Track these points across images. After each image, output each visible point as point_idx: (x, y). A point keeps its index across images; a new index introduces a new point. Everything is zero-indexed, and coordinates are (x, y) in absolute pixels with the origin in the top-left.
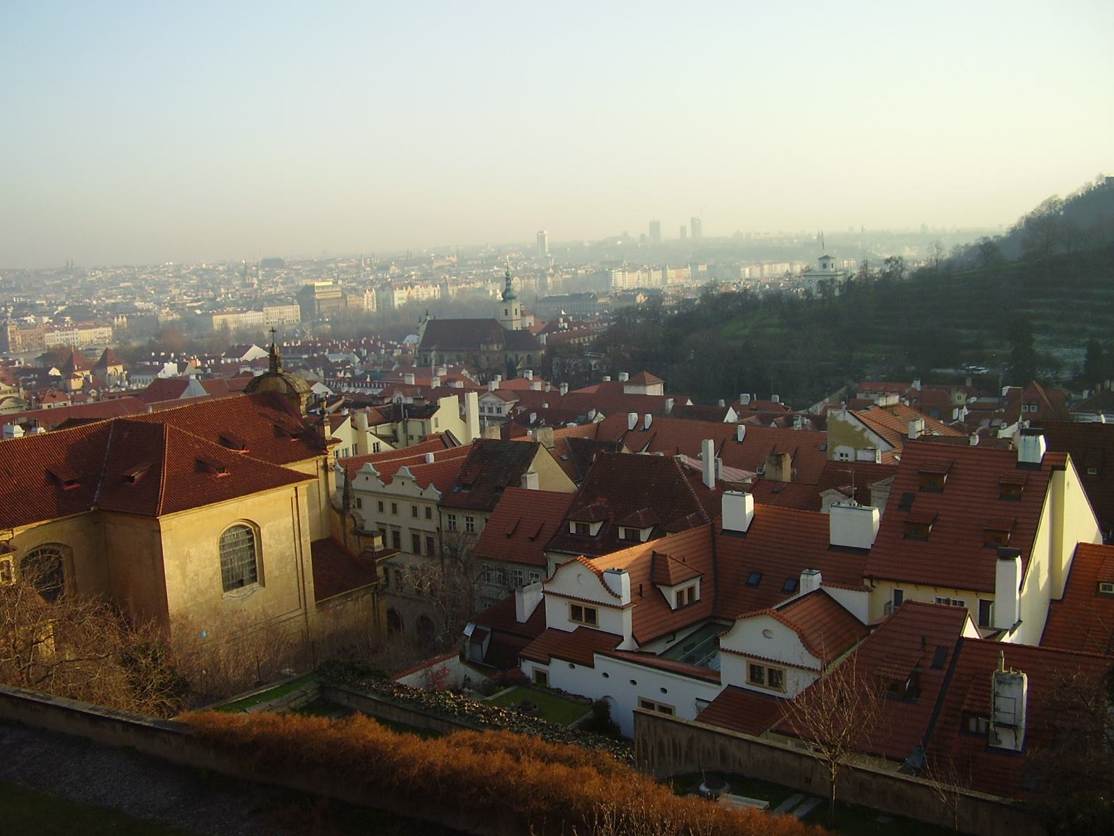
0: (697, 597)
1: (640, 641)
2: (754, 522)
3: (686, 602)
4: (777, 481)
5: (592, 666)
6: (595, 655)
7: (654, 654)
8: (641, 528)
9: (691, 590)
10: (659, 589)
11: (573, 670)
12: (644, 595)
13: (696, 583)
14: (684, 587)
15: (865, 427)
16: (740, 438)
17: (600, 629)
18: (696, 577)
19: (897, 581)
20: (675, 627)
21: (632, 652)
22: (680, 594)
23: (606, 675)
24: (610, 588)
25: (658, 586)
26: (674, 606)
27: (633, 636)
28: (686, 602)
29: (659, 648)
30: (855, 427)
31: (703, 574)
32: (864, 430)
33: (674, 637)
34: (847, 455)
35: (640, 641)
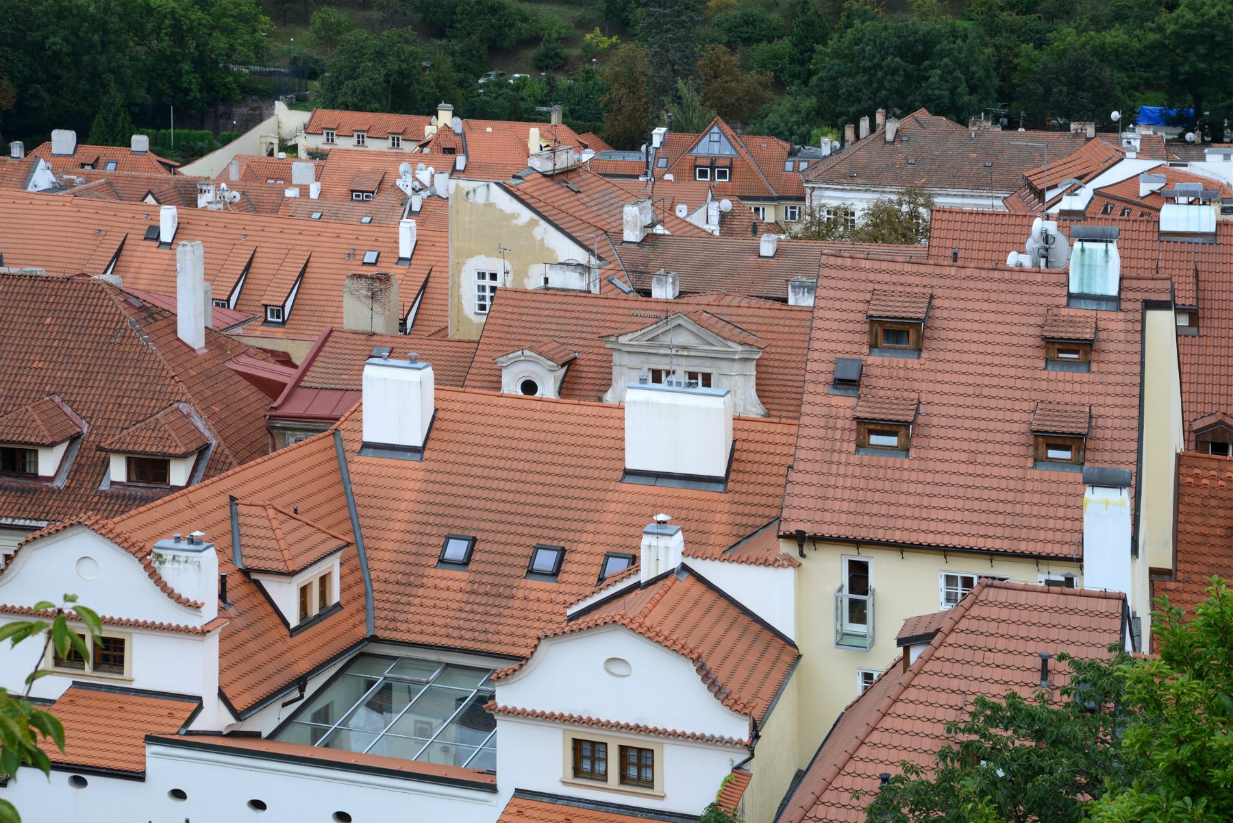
0: (335, 597)
1: (239, 705)
2: (437, 424)
3: (314, 609)
4: (374, 334)
5: (139, 777)
6: (151, 749)
7: (256, 735)
8: (44, 446)
9: (324, 580)
10: (257, 584)
11: (83, 791)
12: (228, 600)
13: (333, 566)
14: (311, 576)
15: (536, 217)
16: (166, 235)
17: (135, 685)
18: (331, 553)
19: (858, 543)
20: (303, 667)
21: (218, 734)
22: (304, 591)
23: (178, 794)
24: (170, 585)
25: (255, 576)
26: (294, 621)
27: (222, 695)
28: (314, 609)
29: (266, 721)
30: (514, 216)
31: (348, 544)
32: (532, 224)
33: (302, 689)
34: (494, 277)
35: (239, 705)
